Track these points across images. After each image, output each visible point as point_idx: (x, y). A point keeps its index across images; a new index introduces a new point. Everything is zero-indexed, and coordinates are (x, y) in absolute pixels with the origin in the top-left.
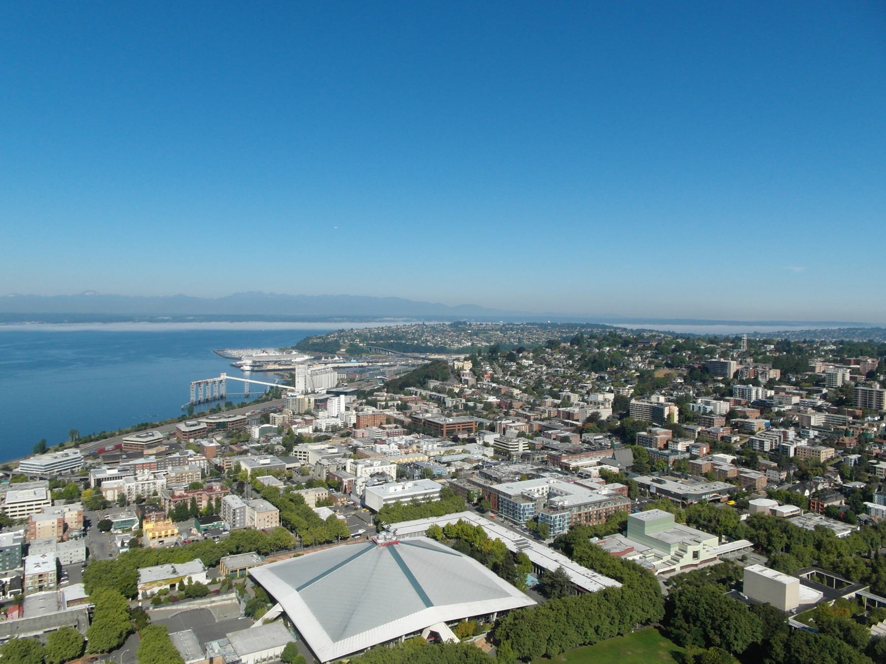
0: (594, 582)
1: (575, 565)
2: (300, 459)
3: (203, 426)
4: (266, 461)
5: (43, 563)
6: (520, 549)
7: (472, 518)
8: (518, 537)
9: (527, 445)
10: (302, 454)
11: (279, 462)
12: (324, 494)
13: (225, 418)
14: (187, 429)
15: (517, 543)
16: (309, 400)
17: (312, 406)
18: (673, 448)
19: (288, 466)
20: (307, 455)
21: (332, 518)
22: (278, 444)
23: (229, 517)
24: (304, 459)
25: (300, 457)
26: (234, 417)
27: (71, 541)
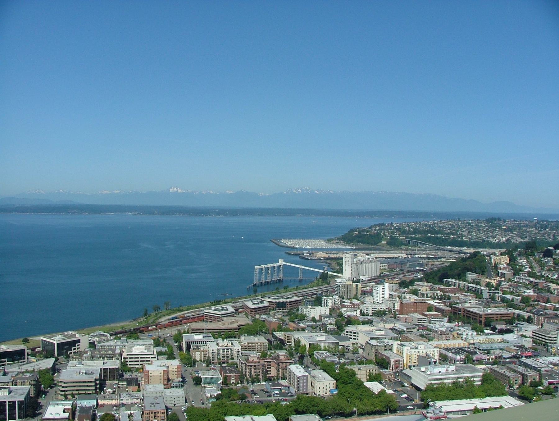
2: (351, 338)
3: (266, 304)
4: (321, 337)
10: (353, 334)
11: (332, 339)
12: (374, 371)
13: (284, 298)
14: (254, 306)
16: (357, 286)
17: (359, 292)
19: (341, 343)
20: (357, 335)
21: (382, 392)
22: (331, 324)
23: (294, 382)
24: (355, 339)
25: (351, 337)
26: (291, 298)
27: (173, 389)
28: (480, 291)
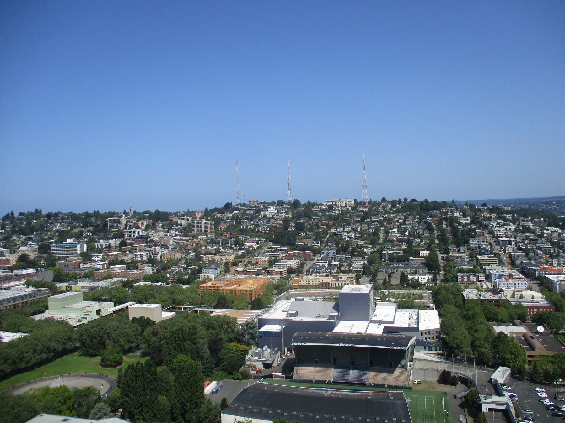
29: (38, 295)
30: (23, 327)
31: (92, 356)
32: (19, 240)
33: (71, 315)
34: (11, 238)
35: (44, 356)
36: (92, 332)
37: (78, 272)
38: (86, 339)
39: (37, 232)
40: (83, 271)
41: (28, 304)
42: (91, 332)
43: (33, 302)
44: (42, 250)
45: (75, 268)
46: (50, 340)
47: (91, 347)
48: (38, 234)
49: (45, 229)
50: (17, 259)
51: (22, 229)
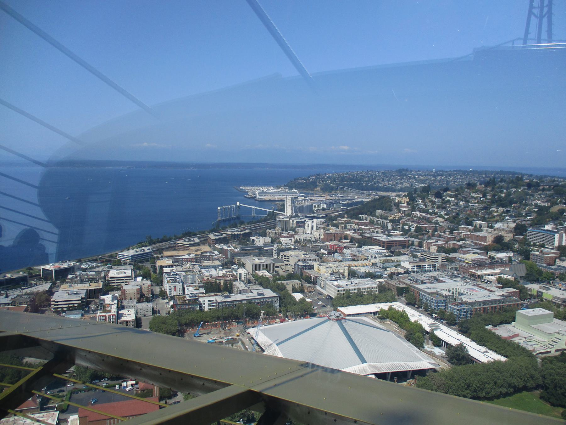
0: (486, 356)
1: (474, 344)
2: (285, 261)
3: (224, 235)
5: (128, 315)
6: (433, 330)
7: (399, 306)
8: (431, 321)
9: (445, 258)
10: (286, 257)
14: (214, 238)
15: (430, 325)
16: (293, 221)
17: (295, 225)
18: (559, 265)
24: (287, 261)
25: (285, 259)
26: (244, 231)
28: (385, 224)
29: (507, 301)
30: (489, 343)
31: (553, 405)
32: (497, 212)
33: (538, 337)
34: (491, 208)
35: (504, 390)
36: (557, 380)
37: (552, 271)
38: (548, 383)
39: (516, 205)
40: (558, 271)
41: (496, 309)
42: (555, 379)
43: (501, 308)
44: (518, 231)
45: (549, 265)
46: (512, 376)
47: (553, 395)
48: (517, 206)
49: (524, 201)
50: (492, 239)
51: (501, 199)
